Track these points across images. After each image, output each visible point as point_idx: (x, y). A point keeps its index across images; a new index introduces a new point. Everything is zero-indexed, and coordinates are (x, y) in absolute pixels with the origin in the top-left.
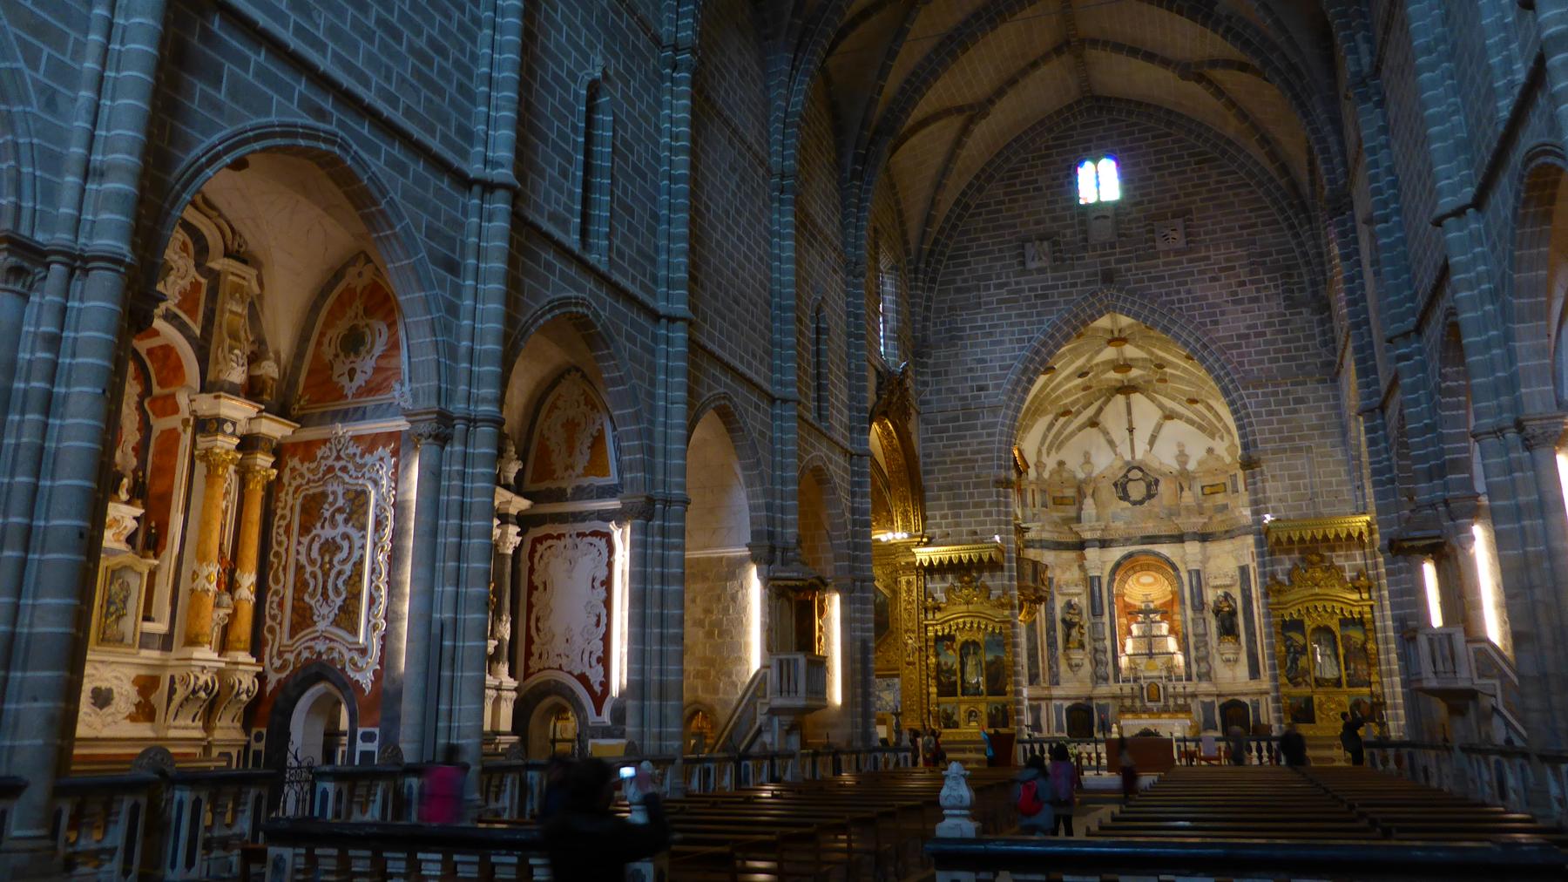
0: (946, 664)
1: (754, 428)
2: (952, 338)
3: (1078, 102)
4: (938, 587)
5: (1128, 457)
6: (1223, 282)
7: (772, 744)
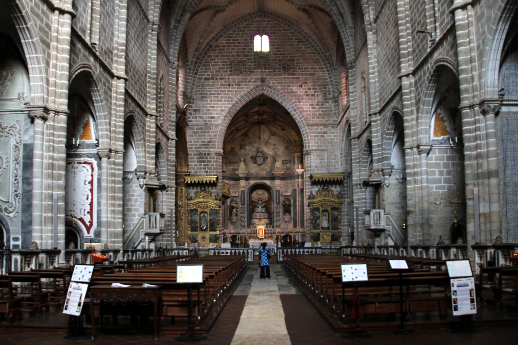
2: (202, 97)
3: (257, 12)
4: (192, 192)
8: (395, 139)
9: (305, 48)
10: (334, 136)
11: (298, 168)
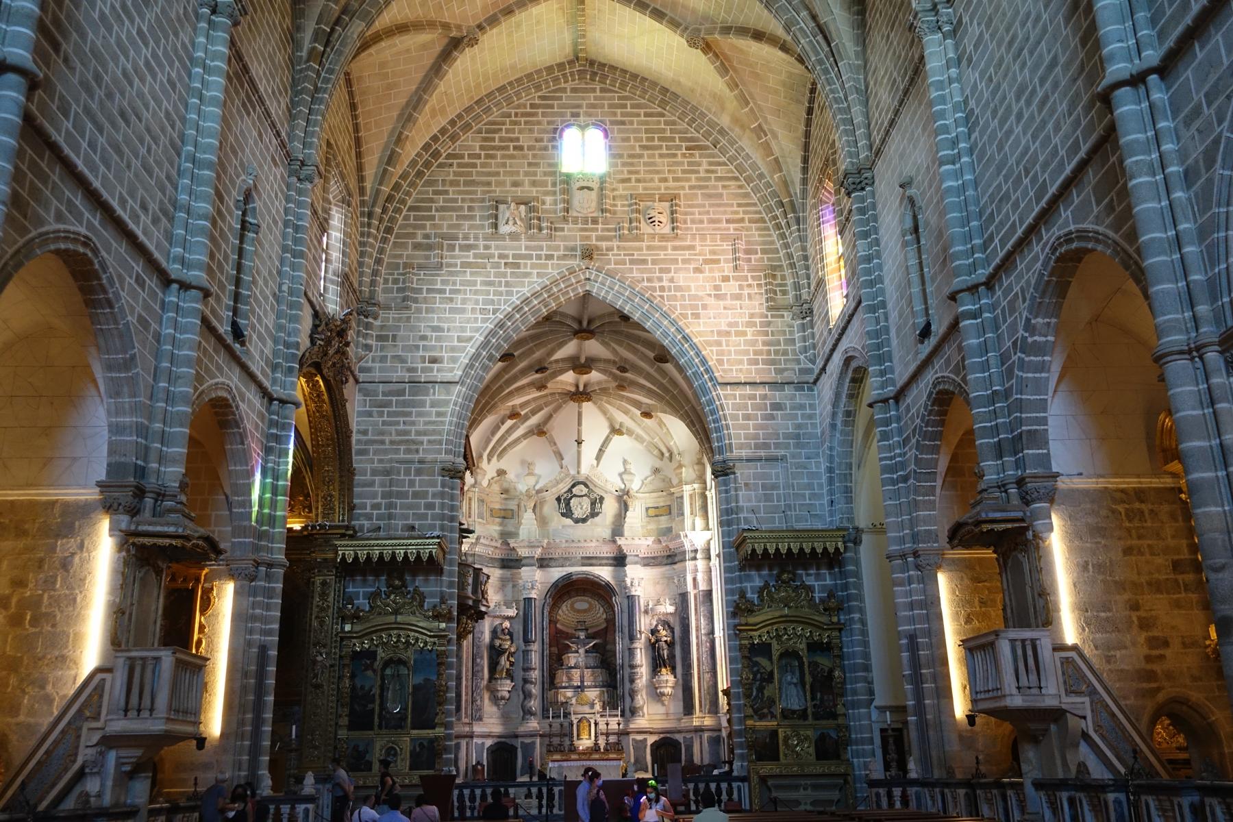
0: (362, 687)
1: (132, 309)
2: (405, 299)
3: (571, 62)
4: (360, 592)
5: (573, 472)
6: (707, 274)
7: (99, 795)
8: (1056, 368)
9: (710, 164)
10: (803, 415)
11: (694, 529)
